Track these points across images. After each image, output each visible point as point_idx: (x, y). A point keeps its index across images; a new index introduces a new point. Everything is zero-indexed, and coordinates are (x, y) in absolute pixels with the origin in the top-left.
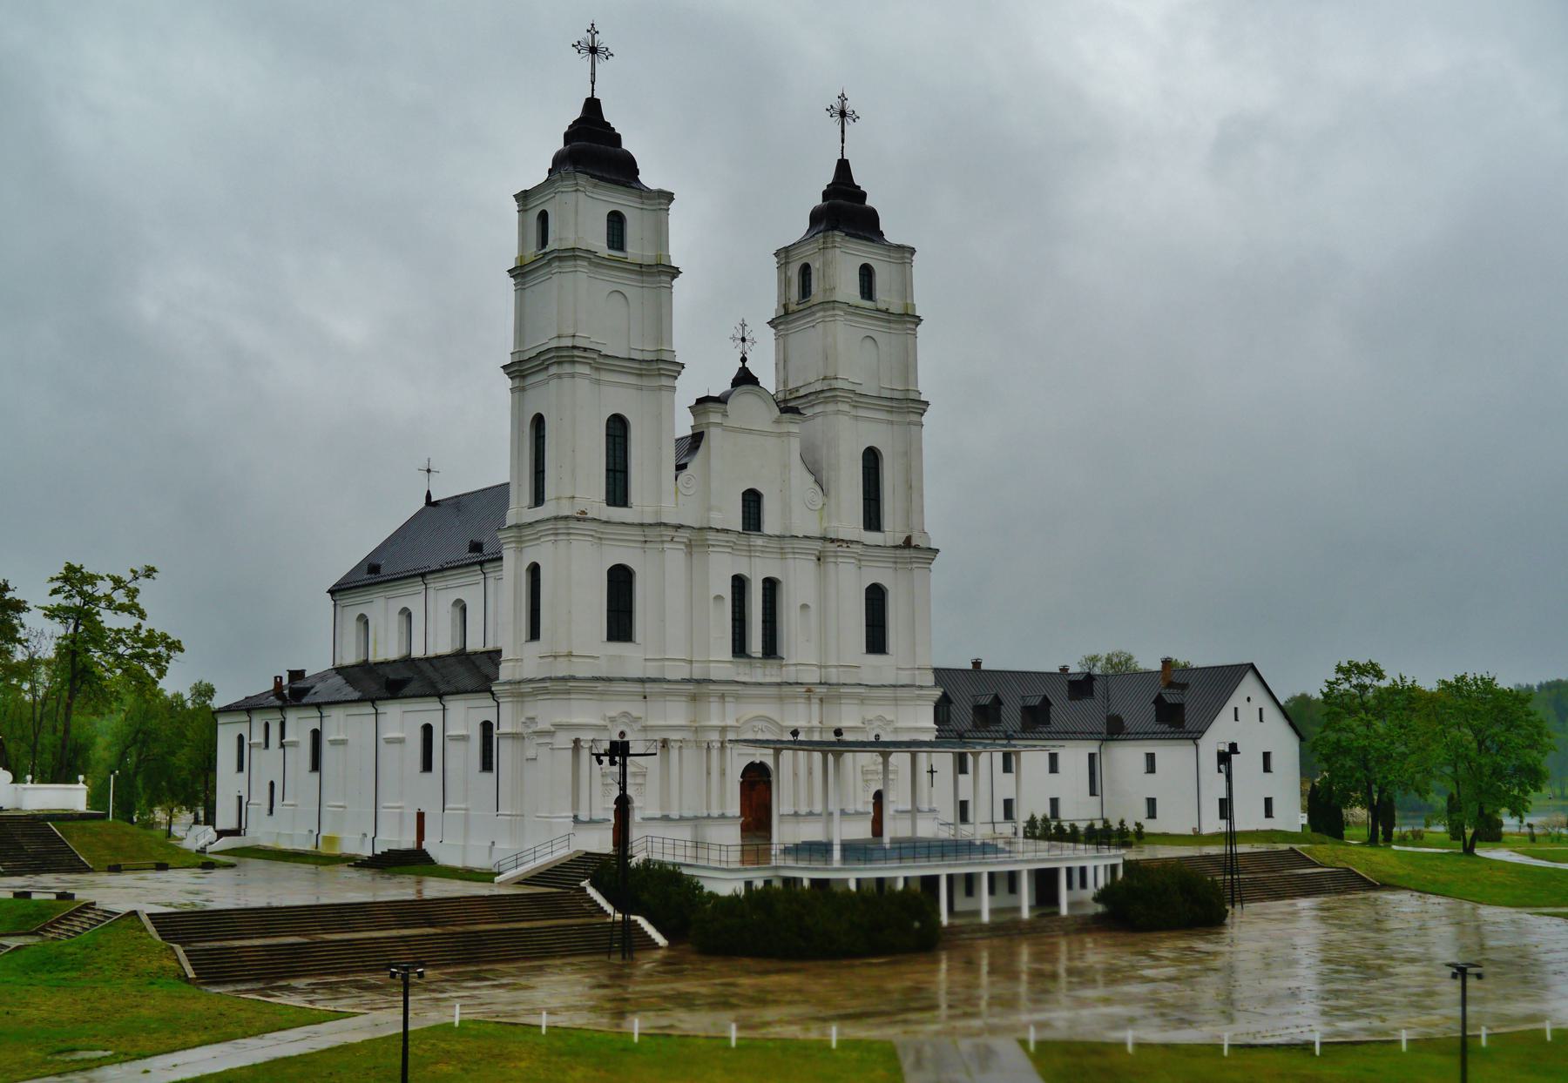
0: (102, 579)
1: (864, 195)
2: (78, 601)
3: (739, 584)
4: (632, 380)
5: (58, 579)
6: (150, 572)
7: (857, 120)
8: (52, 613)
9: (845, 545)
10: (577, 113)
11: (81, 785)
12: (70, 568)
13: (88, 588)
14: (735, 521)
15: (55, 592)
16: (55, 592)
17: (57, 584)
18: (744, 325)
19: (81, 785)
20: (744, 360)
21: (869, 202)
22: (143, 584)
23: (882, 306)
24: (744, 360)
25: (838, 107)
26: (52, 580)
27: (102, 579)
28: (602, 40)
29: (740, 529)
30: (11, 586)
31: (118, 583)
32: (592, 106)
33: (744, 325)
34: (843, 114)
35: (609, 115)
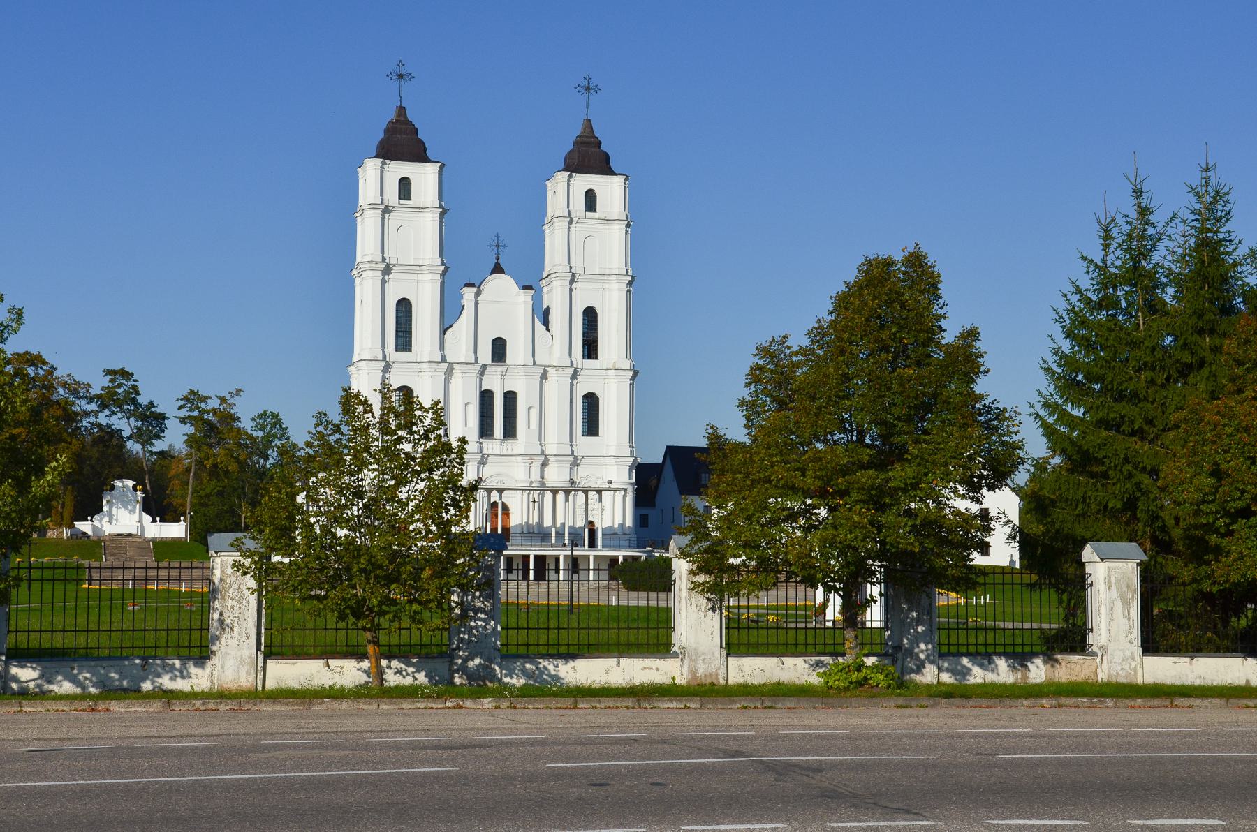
0: (211, 398)
1: (600, 143)
2: (196, 413)
3: (486, 398)
4: (414, 277)
5: (181, 400)
6: (239, 391)
7: (599, 92)
8: (183, 421)
9: (561, 369)
10: (391, 115)
11: (182, 523)
12: (192, 392)
13: (203, 405)
14: (485, 354)
15: (180, 408)
16: (180, 408)
17: (182, 403)
18: (498, 237)
19: (182, 523)
20: (498, 259)
21: (603, 148)
22: (236, 400)
23: (603, 217)
24: (498, 259)
25: (584, 84)
26: (178, 400)
27: (211, 398)
28: (408, 69)
29: (490, 363)
30: (155, 404)
31: (223, 400)
32: (401, 110)
33: (498, 237)
34: (588, 89)
35: (411, 116)
